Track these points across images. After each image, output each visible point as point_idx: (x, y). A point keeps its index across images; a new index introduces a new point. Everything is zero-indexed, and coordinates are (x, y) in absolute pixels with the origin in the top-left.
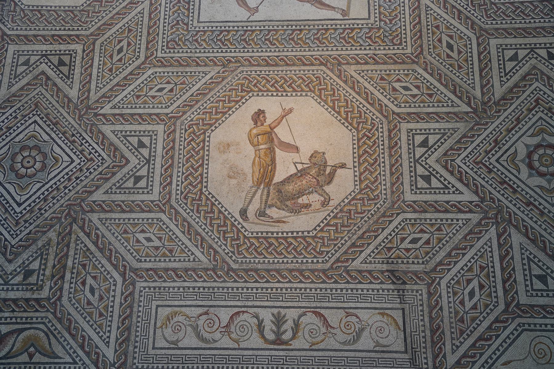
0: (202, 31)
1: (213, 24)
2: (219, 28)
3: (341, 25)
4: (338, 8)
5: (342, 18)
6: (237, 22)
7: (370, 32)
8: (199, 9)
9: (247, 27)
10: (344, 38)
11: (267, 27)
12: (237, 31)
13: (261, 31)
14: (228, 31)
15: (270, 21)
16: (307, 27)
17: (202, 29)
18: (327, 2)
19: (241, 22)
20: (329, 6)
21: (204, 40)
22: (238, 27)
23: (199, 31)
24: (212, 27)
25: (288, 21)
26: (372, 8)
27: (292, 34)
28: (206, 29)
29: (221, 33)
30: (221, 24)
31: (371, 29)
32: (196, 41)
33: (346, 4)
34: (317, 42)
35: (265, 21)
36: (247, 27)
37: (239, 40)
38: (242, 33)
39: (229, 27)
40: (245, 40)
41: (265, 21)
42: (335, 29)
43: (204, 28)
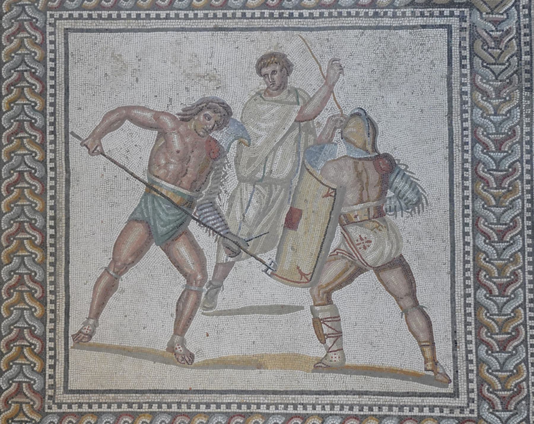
0: (44, 39)
1: (61, 61)
2: (50, 73)
3: (53, 330)
4: (95, 326)
5: (71, 332)
6: (66, 110)
7: (34, 392)
8: (99, 31)
9: (53, 133)
10: (20, 336)
11: (51, 174)
12: (43, 112)
13: (44, 162)
14: (43, 94)
15: (68, 181)
16: (50, 259)
17: (50, 38)
18: (111, 301)
19: (67, 121)
20: (102, 304)
21: (21, 45)
22: (53, 114)
23: (43, 33)
24: (53, 60)
25: (68, 219)
26: (94, 397)
27: (34, 228)
28: (50, 47)
29: (37, 79)
30: (61, 78)
31: (41, 394)
32: (21, 29)
33: (107, 343)
34: (13, 281)
35: (68, 171)
36: (53, 133)
37: (21, 117)
38: (39, 123)
39: (54, 95)
40: (21, 129)
41: (68, 171)
42: (43, 320)
43: (53, 42)
